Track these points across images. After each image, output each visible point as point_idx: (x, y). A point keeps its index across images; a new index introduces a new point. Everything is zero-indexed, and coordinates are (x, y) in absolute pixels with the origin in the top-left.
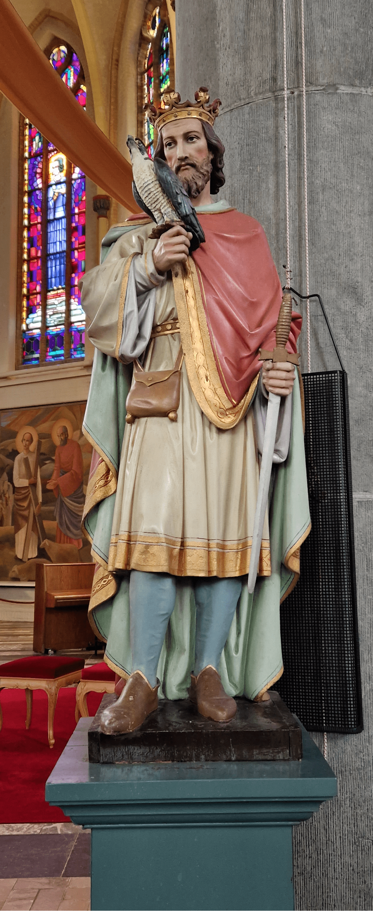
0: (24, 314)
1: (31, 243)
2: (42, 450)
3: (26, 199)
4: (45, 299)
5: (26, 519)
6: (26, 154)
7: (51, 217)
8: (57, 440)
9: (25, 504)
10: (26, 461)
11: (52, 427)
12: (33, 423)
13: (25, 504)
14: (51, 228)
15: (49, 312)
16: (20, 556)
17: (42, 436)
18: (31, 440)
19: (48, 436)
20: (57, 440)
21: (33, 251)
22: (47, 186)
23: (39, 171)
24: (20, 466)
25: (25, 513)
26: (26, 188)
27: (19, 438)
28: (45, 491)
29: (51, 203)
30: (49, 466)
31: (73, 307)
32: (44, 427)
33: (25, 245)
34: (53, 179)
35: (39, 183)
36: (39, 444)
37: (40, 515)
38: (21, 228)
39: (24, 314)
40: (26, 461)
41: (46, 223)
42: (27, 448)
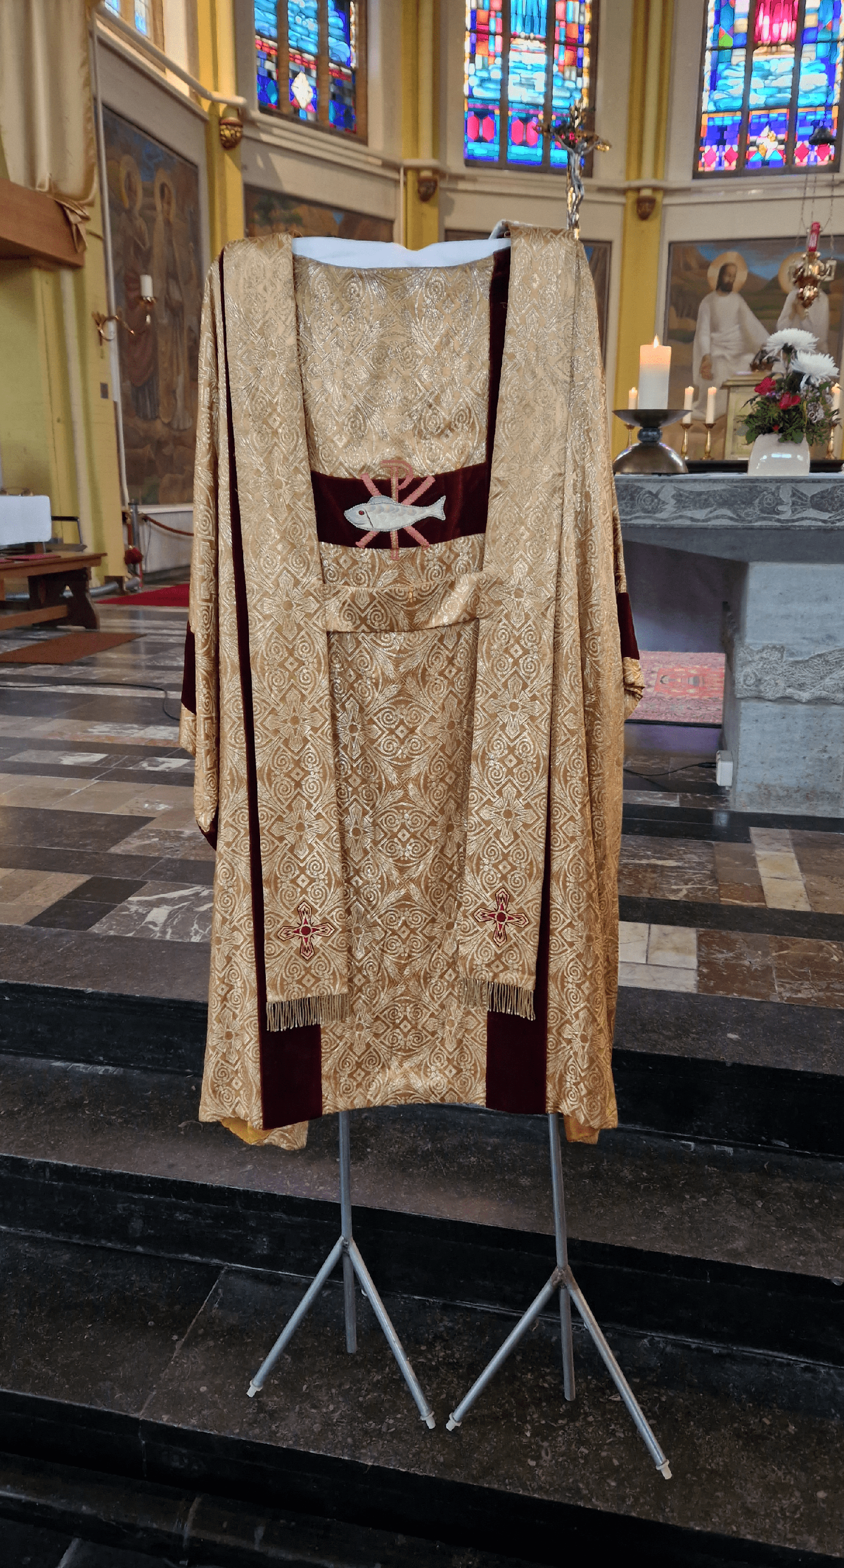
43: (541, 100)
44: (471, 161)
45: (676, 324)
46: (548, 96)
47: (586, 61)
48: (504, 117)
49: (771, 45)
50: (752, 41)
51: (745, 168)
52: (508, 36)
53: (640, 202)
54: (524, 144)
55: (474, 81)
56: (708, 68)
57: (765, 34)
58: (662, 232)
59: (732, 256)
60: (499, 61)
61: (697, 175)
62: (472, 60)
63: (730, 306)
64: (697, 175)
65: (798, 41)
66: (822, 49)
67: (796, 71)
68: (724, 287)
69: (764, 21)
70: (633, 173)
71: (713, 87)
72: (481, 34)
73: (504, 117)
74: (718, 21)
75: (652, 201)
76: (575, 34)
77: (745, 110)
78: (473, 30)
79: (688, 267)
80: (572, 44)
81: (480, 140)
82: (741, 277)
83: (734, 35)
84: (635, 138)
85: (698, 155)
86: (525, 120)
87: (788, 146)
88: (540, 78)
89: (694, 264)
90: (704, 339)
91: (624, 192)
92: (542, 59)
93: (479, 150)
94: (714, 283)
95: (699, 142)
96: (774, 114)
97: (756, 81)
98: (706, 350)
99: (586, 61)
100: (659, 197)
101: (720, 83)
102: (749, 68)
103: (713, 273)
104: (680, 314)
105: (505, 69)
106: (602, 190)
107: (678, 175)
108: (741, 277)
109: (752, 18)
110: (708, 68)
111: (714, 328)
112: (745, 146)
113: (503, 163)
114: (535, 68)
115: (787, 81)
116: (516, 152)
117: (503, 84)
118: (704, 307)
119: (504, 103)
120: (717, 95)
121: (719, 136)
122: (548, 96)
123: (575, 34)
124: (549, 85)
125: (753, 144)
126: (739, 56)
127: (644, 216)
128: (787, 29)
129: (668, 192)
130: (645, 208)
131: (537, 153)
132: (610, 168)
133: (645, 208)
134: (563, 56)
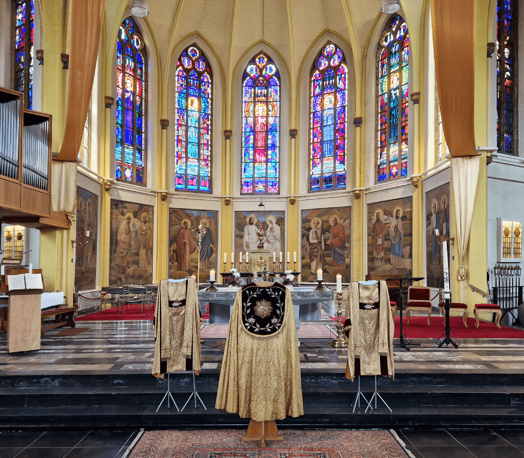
0: (311, 168)
1: (315, 136)
2: (324, 228)
3: (312, 116)
4: (322, 162)
5: (316, 257)
6: (312, 95)
7: (325, 124)
8: (332, 223)
9: (316, 250)
10: (316, 232)
11: (329, 218)
12: (319, 216)
13: (316, 250)
14: (325, 129)
15: (324, 167)
16: (313, 272)
17: (323, 222)
18: (319, 223)
19: (327, 222)
20: (332, 223)
21: (316, 139)
22: (323, 110)
23: (319, 103)
24: (312, 234)
25: (316, 254)
26: (312, 110)
27: (312, 222)
28: (325, 245)
29: (325, 118)
30: (328, 235)
31: (336, 165)
32: (325, 218)
33: (311, 136)
34: (326, 107)
35: (318, 108)
36: (323, 225)
37: (323, 255)
38: (310, 129)
39: (311, 168)
40: (316, 232)
41: (322, 127)
42: (316, 227)
43: (197, 174)
44: (177, 189)
45: (238, 233)
46: (199, 173)
47: (209, 164)
48: (186, 178)
49: (260, 162)
50: (254, 161)
51: (254, 193)
52: (187, 158)
53: (226, 201)
54: (192, 185)
55: (178, 169)
56: (243, 167)
57: (258, 160)
58: (232, 209)
59: (252, 215)
60: (185, 164)
61: (241, 194)
62: (177, 164)
63: (253, 229)
64: (241, 194)
65: (267, 161)
66: (273, 164)
67: (266, 169)
68: (251, 223)
69: (257, 156)
70: (224, 194)
71: (245, 172)
72: (180, 157)
73: (186, 178)
74: (245, 156)
75: (229, 201)
76: (206, 157)
77: (253, 177)
78: (177, 156)
79: (240, 218)
80: (205, 160)
81: (180, 184)
82: (255, 221)
83: (250, 159)
84: (224, 185)
85: (242, 189)
86: (192, 179)
87: (266, 187)
88: (197, 168)
89: (242, 217)
90: (246, 237)
91: (221, 198)
92: (197, 164)
93: (179, 186)
94: (248, 222)
95: (242, 185)
96: (261, 179)
97: (256, 171)
98: (247, 240)
99: (209, 164)
100: (231, 199)
101: (246, 171)
102: (254, 167)
103: (248, 220)
104: (239, 230)
105: (186, 166)
106: (214, 197)
107: (236, 194)
108: (255, 221)
109: (254, 155)
110: (243, 167)
111: (249, 234)
112: (254, 187)
113: (187, 190)
114: (195, 166)
115: (264, 171)
116: (190, 187)
117: (186, 170)
118: (246, 229)
119: (186, 174)
120: (246, 174)
121: (247, 184)
122: (199, 173)
123: (206, 157)
124: (199, 170)
125: (256, 186)
126: (251, 164)
127: (227, 205)
128: (263, 159)
129: (233, 198)
130: (227, 202)
131: (196, 188)
132: (217, 191)
133: (227, 202)
134: (203, 163)
